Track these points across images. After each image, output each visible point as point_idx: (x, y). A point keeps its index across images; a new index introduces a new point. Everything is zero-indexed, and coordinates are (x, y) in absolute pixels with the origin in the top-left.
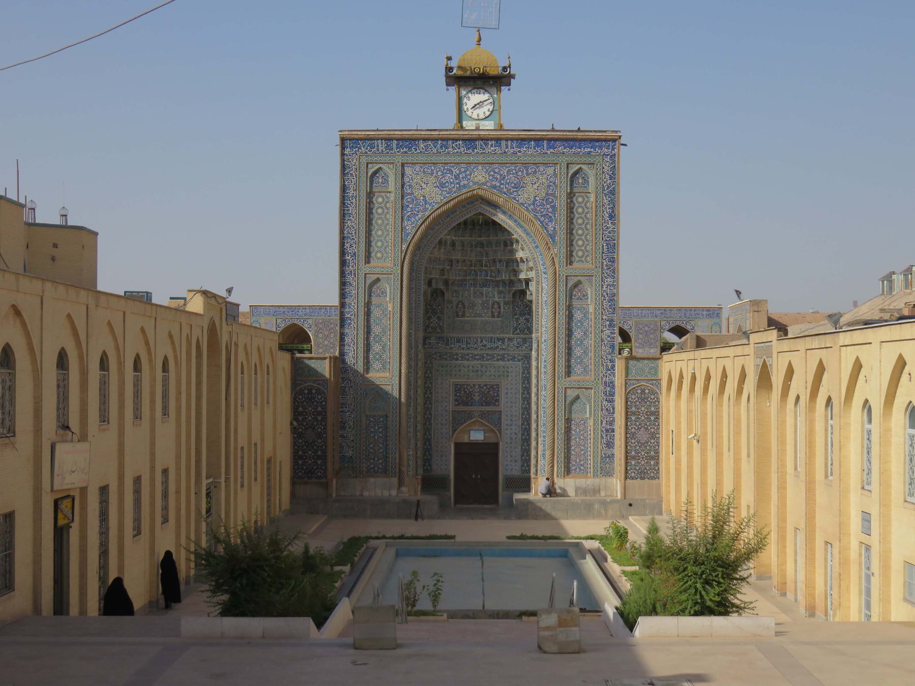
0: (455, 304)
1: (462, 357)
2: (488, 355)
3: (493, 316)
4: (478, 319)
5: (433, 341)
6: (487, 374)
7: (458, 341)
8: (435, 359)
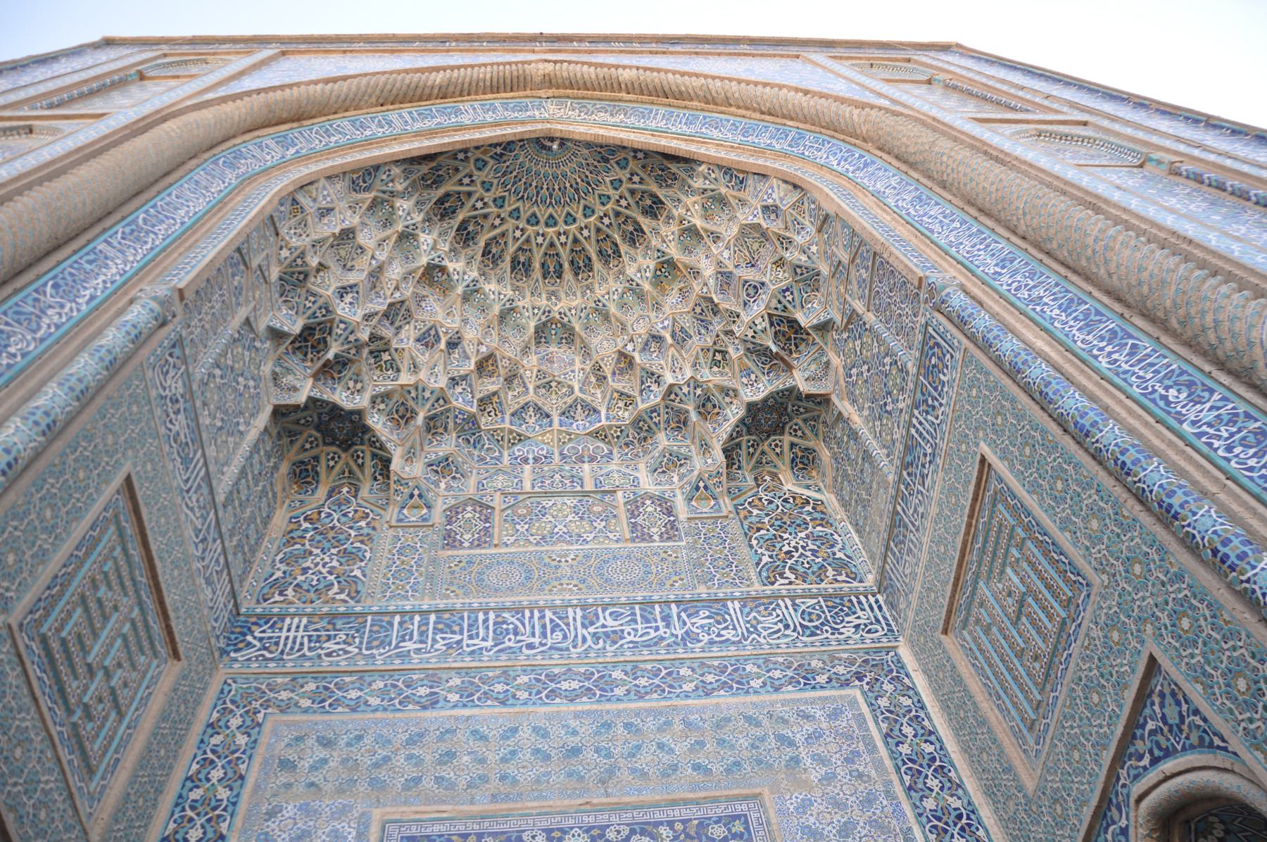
0: (439, 507)
2: (634, 670)
5: (293, 630)
6: (643, 760)
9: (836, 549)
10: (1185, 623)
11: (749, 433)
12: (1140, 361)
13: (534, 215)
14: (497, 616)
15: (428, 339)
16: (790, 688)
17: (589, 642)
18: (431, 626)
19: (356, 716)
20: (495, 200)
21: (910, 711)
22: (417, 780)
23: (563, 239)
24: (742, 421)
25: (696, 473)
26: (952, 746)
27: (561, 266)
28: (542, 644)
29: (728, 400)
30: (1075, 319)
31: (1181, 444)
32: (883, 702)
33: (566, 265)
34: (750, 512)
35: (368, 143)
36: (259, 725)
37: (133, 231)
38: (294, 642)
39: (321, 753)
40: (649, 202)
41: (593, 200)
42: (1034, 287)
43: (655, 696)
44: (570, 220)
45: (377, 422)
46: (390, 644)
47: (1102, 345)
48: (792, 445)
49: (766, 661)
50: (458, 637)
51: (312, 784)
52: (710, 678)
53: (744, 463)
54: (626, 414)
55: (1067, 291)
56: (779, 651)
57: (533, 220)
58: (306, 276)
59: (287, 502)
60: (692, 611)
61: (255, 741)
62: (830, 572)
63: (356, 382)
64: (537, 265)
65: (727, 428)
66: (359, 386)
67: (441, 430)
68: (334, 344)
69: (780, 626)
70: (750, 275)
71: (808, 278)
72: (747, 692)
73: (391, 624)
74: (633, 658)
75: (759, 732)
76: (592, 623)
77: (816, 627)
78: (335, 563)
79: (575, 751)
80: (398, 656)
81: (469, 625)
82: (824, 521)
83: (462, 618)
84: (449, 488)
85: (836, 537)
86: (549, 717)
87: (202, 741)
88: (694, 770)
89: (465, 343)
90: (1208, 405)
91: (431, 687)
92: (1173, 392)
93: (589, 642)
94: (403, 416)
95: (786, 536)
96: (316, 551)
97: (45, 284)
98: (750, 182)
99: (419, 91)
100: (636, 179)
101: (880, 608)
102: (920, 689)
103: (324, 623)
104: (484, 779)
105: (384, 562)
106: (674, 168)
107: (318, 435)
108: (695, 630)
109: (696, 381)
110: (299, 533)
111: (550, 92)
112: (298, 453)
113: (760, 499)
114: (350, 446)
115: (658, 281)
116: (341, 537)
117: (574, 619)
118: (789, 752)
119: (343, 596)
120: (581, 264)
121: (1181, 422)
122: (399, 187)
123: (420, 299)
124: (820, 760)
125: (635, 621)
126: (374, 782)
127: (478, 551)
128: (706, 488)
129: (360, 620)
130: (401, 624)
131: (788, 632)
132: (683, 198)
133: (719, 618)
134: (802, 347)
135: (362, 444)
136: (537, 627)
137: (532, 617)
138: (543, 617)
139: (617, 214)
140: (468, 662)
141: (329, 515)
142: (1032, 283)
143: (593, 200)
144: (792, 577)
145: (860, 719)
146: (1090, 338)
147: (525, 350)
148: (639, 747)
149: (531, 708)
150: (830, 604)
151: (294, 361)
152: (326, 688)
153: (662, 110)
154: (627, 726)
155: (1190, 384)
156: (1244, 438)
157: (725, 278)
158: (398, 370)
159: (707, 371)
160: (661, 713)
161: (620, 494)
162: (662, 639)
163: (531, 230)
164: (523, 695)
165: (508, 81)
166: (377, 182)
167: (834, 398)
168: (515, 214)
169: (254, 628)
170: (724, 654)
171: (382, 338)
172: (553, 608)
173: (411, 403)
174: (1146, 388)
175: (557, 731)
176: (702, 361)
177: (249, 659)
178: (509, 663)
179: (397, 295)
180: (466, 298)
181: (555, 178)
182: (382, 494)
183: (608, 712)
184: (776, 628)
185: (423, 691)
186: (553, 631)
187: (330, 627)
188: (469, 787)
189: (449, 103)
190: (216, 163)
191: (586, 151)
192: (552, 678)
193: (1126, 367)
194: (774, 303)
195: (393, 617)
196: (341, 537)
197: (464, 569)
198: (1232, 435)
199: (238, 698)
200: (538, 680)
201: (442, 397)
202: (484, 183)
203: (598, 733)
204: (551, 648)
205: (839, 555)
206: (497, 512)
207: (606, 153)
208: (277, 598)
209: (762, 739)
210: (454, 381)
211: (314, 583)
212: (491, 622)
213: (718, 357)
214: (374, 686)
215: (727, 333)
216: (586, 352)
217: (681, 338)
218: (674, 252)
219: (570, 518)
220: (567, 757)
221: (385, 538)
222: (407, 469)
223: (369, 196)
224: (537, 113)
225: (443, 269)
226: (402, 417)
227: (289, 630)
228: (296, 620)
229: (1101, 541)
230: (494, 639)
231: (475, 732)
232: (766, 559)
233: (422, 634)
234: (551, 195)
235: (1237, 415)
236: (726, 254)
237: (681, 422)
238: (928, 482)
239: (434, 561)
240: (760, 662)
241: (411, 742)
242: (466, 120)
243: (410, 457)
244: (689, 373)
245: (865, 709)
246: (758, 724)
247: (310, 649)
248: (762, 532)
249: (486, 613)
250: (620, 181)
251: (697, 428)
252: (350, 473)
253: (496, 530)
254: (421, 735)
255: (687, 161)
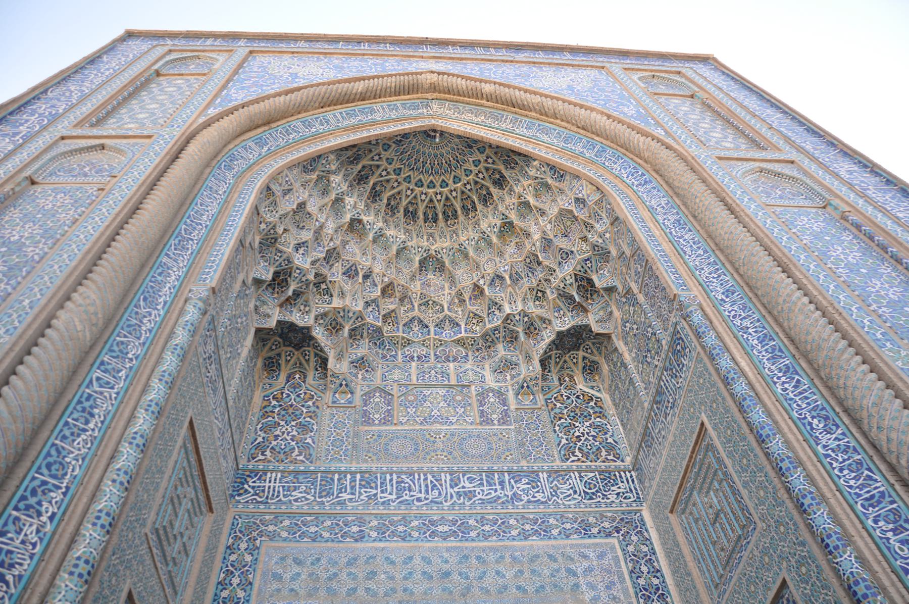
1: (382, 531)
2: (482, 520)
3: (489, 422)
4: (437, 426)
6: (488, 582)
7: (367, 484)
8: (272, 537)
9: (608, 436)
10: (804, 570)
11: (557, 349)
12: (800, 393)
13: (420, 180)
14: (398, 477)
15: (350, 273)
16: (575, 536)
17: (455, 498)
18: (358, 482)
19: (315, 544)
20: (395, 170)
21: (646, 556)
22: (354, 590)
23: (439, 197)
24: (553, 342)
25: (522, 376)
26: (669, 580)
27: (437, 215)
28: (427, 499)
29: (544, 325)
30: (766, 351)
31: (815, 459)
32: (631, 549)
33: (440, 216)
34: (555, 405)
35: (316, 137)
36: (258, 548)
37: (180, 241)
38: (274, 491)
39: (297, 569)
40: (498, 176)
41: (460, 173)
42: (745, 318)
43: (494, 538)
44: (444, 184)
45: (319, 333)
46: (333, 495)
47: (780, 374)
48: (584, 358)
49: (562, 516)
50: (374, 491)
51: (292, 590)
52: (527, 527)
53: (552, 369)
54: (478, 328)
55: (764, 327)
56: (570, 510)
57: (420, 184)
58: (276, 240)
59: (261, 384)
60: (517, 478)
61: (256, 559)
62: (604, 453)
63: (305, 306)
64: (421, 214)
65: (543, 345)
66: (307, 309)
67: (358, 337)
68: (292, 283)
69: (571, 491)
70: (562, 243)
71: (601, 253)
72: (550, 538)
73: (333, 480)
74: (482, 511)
75: (555, 566)
76: (456, 485)
77: (593, 493)
78: (295, 433)
79: (447, 574)
80: (339, 503)
81: (382, 483)
82: (602, 415)
83: (376, 478)
84: (364, 378)
85: (608, 426)
86: (432, 550)
87: (225, 558)
88: (517, 589)
89: (374, 275)
90: (834, 436)
91: (360, 526)
92: (815, 421)
93: (455, 498)
94: (334, 327)
95: (577, 424)
96: (282, 423)
97: (139, 300)
98: (567, 178)
99: (347, 97)
100: (490, 160)
101: (633, 481)
102: (654, 541)
103: (291, 478)
104: (394, 590)
105: (326, 433)
106: (516, 158)
107: (281, 340)
108: (520, 493)
109: (525, 312)
110: (269, 409)
111: (435, 95)
112: (268, 352)
113: (562, 395)
114: (301, 347)
115: (501, 235)
116: (298, 413)
117: (446, 481)
118: (573, 580)
119: (301, 458)
120: (450, 214)
121: (818, 444)
122: (333, 168)
123: (345, 243)
124: (592, 587)
125: (482, 484)
126: (329, 590)
127: (384, 428)
128: (528, 387)
129: (314, 476)
130: (339, 480)
131: (576, 496)
132: (522, 180)
133: (534, 484)
134: (595, 296)
135: (309, 346)
136: (423, 486)
137: (419, 479)
138: (426, 479)
139: (476, 183)
140: (381, 510)
141: (288, 396)
142: (743, 315)
143: (460, 173)
144: (580, 455)
145: (616, 559)
146: (773, 367)
147: (413, 278)
148: (484, 573)
149: (420, 544)
150: (602, 477)
151: (267, 296)
152: (296, 524)
153: (511, 116)
154: (478, 558)
155: (826, 418)
156: (850, 465)
157: (547, 243)
158: (332, 296)
159: (531, 304)
160: (498, 550)
161: (473, 388)
162: (499, 498)
163: (418, 190)
164: (415, 534)
165: (406, 88)
166: (320, 165)
167: (613, 336)
168: (408, 179)
169: (248, 479)
170: (536, 510)
171: (321, 275)
172: (432, 473)
173: (340, 320)
174: (801, 414)
175: (436, 560)
176: (529, 296)
177: (247, 502)
178: (406, 512)
179: (331, 244)
180: (374, 241)
181: (436, 156)
182: (322, 382)
183: (466, 548)
184: (569, 493)
185: (355, 529)
186: (432, 490)
187: (295, 480)
188: (385, 595)
189: (366, 104)
190: (219, 168)
191: (457, 140)
192: (432, 523)
193: (791, 395)
194: (579, 268)
195: (334, 475)
196: (298, 413)
197: (375, 440)
198: (844, 460)
199: (243, 529)
200: (424, 524)
201: (360, 317)
202: (388, 159)
203: (460, 562)
204: (431, 502)
205: (610, 440)
206: (395, 398)
207: (470, 143)
208: (261, 457)
209: (558, 571)
210: (367, 304)
211: (283, 447)
212: (394, 482)
213: (539, 295)
214: (325, 524)
215: (546, 280)
216: (452, 281)
217: (516, 278)
218: (513, 216)
219: (441, 405)
220: (442, 578)
221: (326, 414)
222: (338, 366)
223: (314, 176)
224: (425, 111)
225: (360, 221)
226: (334, 328)
227: (270, 482)
228: (274, 475)
229: (764, 504)
230: (397, 494)
231: (387, 559)
232: (564, 441)
233: (353, 487)
234: (432, 168)
235: (848, 447)
236: (549, 226)
237: (513, 338)
238: (669, 418)
239: (356, 434)
240: (558, 517)
241: (349, 564)
242: (377, 117)
243: (340, 357)
244: (520, 308)
245: (620, 553)
246: (556, 561)
247: (284, 495)
248: (563, 421)
249: (391, 475)
250: (479, 161)
251: (524, 346)
252: (300, 364)
253: (395, 412)
254: (355, 559)
255: (527, 158)
